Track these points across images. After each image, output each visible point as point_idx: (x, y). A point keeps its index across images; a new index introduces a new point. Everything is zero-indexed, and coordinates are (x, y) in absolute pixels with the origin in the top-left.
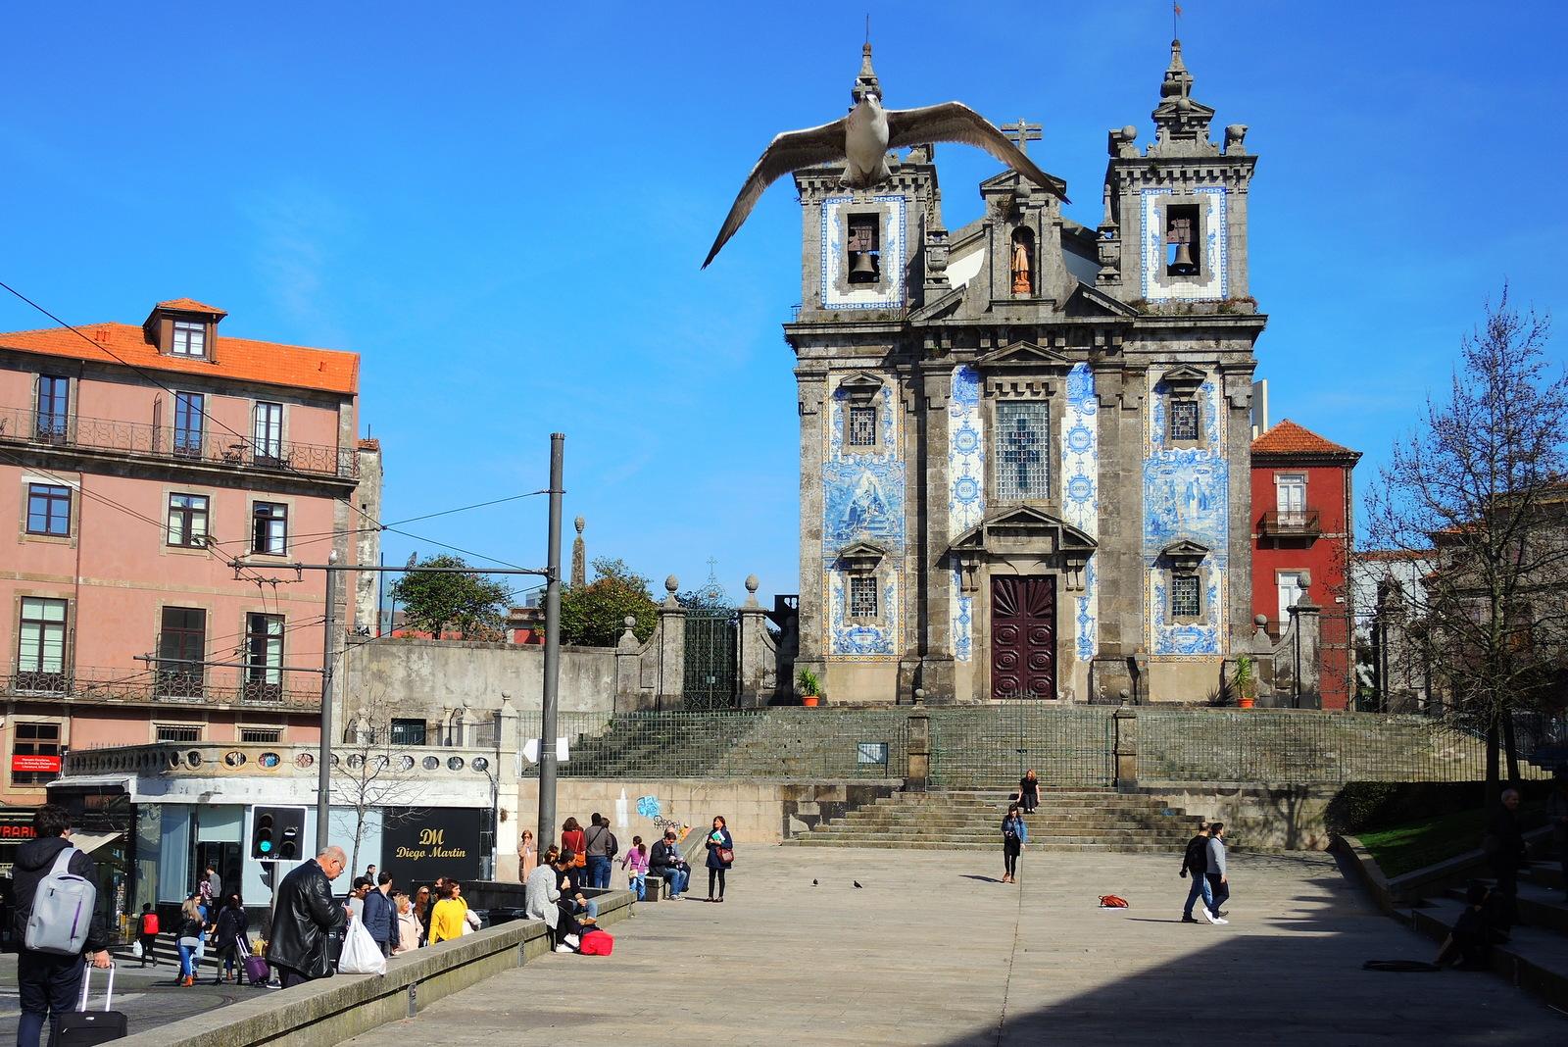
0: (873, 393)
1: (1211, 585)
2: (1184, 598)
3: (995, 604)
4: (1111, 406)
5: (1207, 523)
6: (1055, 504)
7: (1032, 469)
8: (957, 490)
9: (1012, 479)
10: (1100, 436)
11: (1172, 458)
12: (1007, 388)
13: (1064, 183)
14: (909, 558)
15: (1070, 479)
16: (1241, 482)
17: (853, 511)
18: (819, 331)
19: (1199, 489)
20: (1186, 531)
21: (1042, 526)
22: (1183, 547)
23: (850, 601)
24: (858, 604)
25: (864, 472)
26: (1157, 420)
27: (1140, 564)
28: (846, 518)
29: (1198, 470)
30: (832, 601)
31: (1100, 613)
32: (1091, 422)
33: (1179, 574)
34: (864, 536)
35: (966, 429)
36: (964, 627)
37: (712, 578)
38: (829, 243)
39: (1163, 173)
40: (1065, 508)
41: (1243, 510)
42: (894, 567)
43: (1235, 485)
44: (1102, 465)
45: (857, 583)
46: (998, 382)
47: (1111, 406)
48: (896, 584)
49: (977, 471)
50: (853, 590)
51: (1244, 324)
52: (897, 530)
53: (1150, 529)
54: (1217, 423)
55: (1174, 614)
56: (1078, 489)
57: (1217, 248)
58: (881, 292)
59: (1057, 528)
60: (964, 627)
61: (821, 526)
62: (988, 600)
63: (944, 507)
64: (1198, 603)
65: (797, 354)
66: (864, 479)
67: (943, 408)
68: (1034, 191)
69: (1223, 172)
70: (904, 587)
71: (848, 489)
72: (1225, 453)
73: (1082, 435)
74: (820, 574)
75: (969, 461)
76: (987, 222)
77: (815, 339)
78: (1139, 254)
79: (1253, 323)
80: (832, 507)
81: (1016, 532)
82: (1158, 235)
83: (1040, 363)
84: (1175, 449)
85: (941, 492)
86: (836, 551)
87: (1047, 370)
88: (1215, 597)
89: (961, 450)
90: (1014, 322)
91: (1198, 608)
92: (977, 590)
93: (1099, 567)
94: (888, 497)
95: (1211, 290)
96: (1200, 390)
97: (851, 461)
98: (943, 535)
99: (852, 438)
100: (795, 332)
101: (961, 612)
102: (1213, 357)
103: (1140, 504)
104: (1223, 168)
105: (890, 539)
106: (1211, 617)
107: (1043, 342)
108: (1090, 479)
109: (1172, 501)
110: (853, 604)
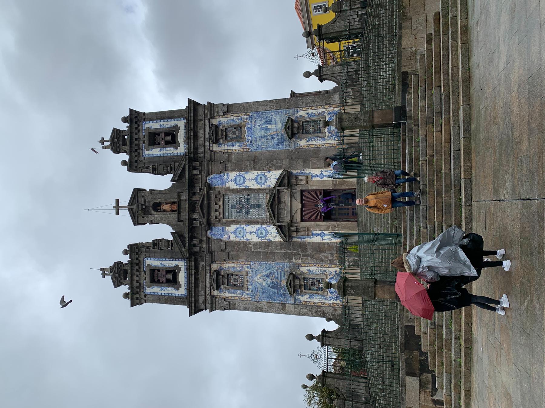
0: (220, 275)
1: (306, 116)
2: (313, 128)
3: (315, 220)
4: (225, 166)
5: (278, 120)
6: (267, 191)
7: (253, 202)
8: (262, 237)
9: (257, 211)
10: (238, 171)
11: (249, 138)
12: (217, 213)
13: (135, 189)
14: (294, 261)
15: (257, 184)
16: (260, 105)
17: (273, 287)
18: (193, 299)
19: (263, 124)
20: (281, 129)
21: (276, 197)
22: (288, 130)
23: (315, 292)
24: (317, 287)
25: (255, 281)
26: (233, 146)
27: (297, 150)
28: (276, 291)
29: (255, 126)
30: (315, 300)
31: (319, 168)
32: (232, 175)
33: (301, 131)
34: (284, 282)
35: (235, 232)
36: (326, 235)
37: (308, 356)
38: (161, 292)
39: (136, 148)
40: (270, 186)
41: (272, 104)
42: (299, 268)
43: (261, 108)
44: (251, 170)
45: (307, 287)
46: (214, 218)
47: (225, 166)
48: (307, 268)
49: (253, 228)
50: (310, 289)
51: (192, 109)
52: (281, 266)
53: (281, 146)
54: (235, 118)
55: (320, 132)
56: (261, 180)
57: (165, 123)
58: (180, 269)
59: (278, 190)
60: (326, 235)
61: (279, 303)
62: (313, 223)
63: (270, 243)
64: (315, 121)
65: (204, 310)
66: (258, 281)
67: (226, 243)
68: (138, 202)
69: (136, 123)
70: (308, 265)
71: (263, 289)
72: (247, 114)
73: (238, 179)
74: (302, 305)
75: (249, 231)
76: (150, 222)
77: (196, 301)
78: (167, 156)
79: (192, 105)
80: (271, 298)
81: (278, 209)
82: (160, 149)
83: (206, 199)
84: (245, 136)
85: (263, 245)
86: (290, 297)
87: (209, 195)
88: (312, 113)
89: (244, 235)
90: (187, 210)
91: (317, 121)
92: (308, 228)
93: (297, 169)
94: (267, 269)
95: (181, 123)
96: (221, 127)
97: (250, 287)
98: (282, 244)
99: (240, 287)
100: (193, 311)
101: (319, 236)
102: (207, 122)
103: (269, 151)
104: (135, 123)
105: (286, 270)
106: (320, 114)
107: (197, 198)
108: (257, 175)
109: (268, 137)
110: (317, 290)
